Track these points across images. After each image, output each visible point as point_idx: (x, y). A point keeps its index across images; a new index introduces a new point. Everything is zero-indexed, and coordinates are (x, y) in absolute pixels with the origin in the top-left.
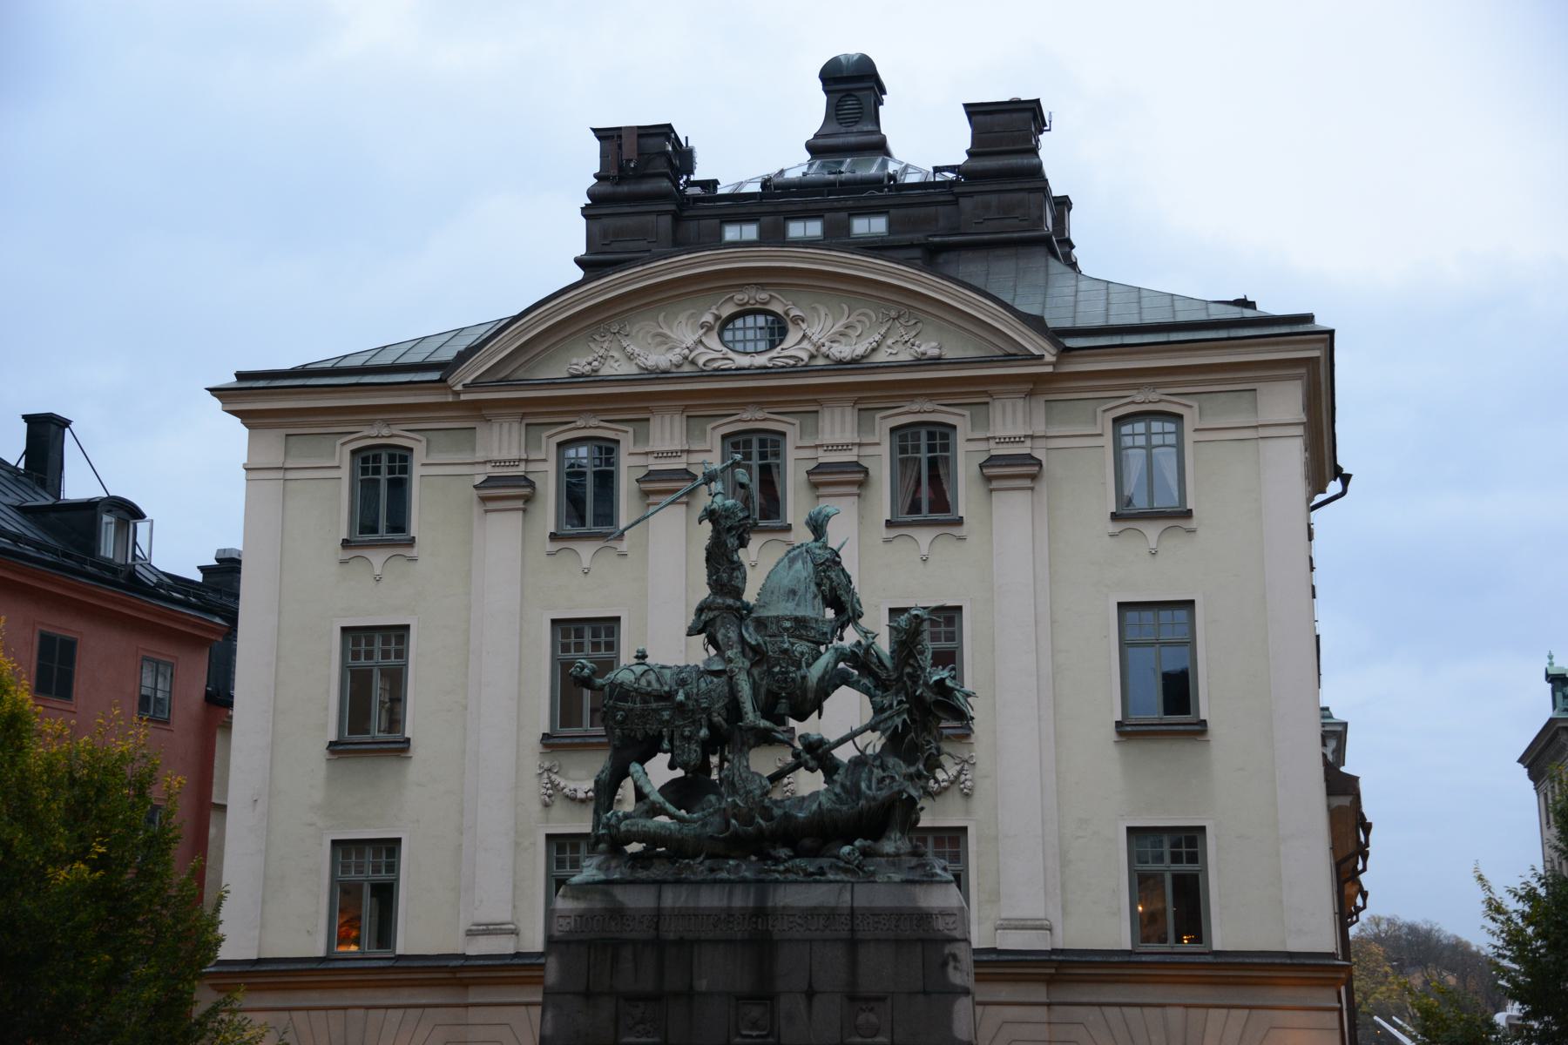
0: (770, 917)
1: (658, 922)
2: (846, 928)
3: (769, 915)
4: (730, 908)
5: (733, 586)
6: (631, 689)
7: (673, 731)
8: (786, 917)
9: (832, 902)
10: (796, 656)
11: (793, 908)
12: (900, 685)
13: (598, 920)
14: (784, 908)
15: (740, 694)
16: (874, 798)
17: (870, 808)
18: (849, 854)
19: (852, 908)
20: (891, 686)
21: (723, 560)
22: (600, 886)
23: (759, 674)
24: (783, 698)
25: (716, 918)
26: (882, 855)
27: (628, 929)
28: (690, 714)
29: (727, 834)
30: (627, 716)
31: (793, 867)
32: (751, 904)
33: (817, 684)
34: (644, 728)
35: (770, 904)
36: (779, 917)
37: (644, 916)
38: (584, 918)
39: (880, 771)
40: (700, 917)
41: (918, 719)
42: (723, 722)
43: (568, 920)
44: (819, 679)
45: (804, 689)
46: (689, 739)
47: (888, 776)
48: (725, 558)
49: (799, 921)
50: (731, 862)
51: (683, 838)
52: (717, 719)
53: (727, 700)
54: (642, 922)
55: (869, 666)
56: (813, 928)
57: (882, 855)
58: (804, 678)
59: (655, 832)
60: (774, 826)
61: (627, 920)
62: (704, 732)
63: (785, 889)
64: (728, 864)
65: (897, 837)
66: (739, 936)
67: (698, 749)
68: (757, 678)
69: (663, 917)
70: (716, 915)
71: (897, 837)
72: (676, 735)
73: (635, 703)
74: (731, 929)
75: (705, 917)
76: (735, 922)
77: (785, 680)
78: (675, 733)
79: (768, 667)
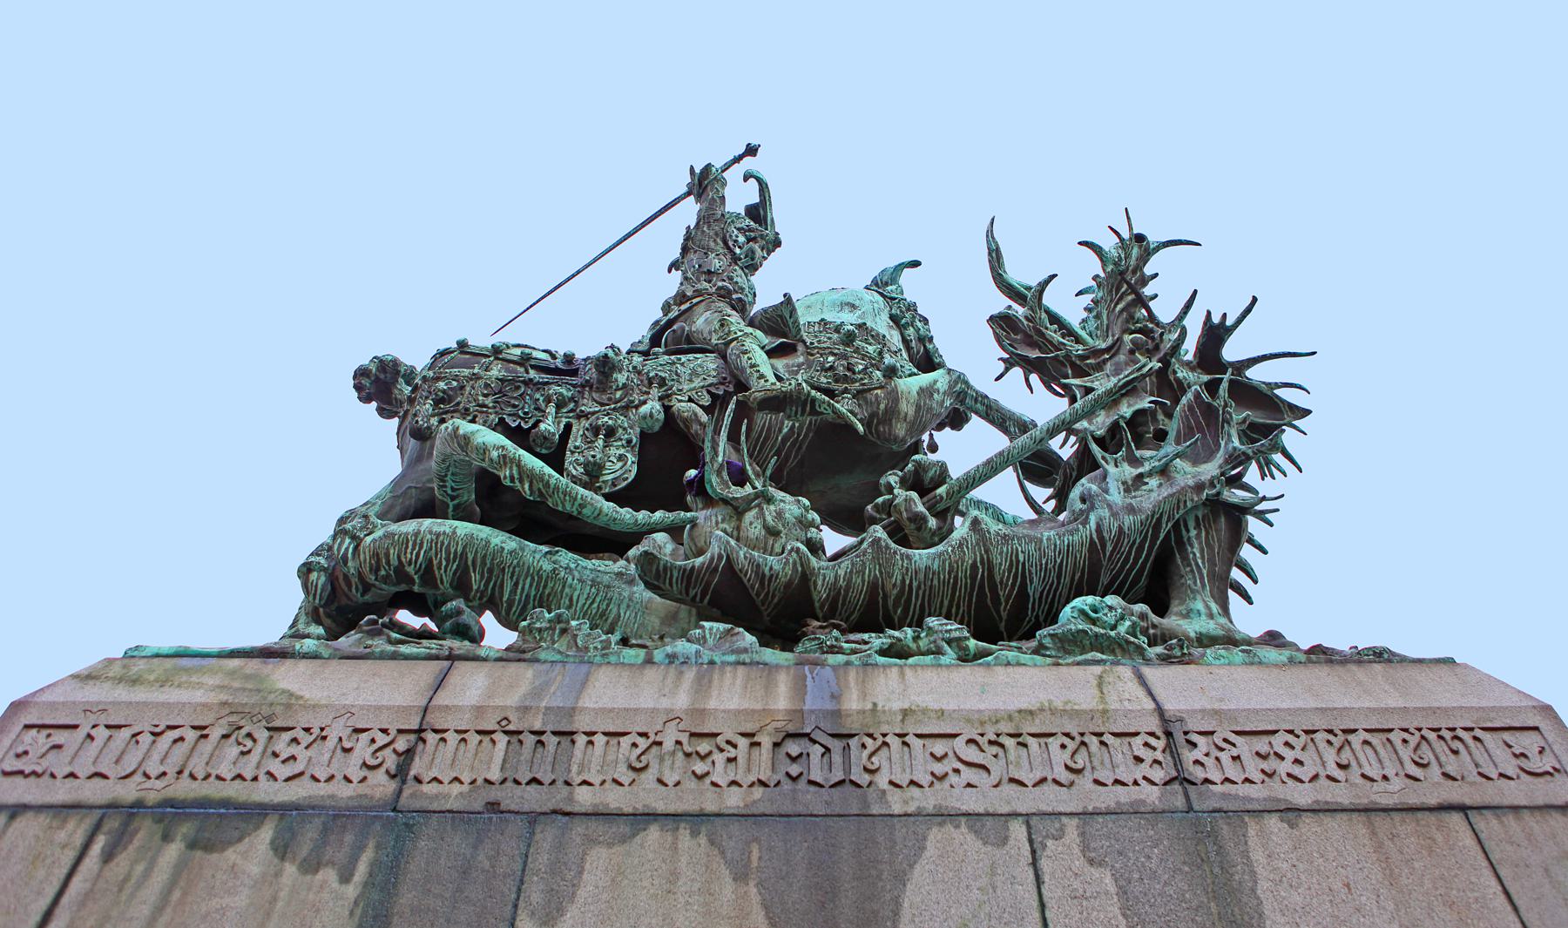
0: (853, 742)
1: (409, 753)
2: (1158, 775)
3: (852, 736)
4: (699, 713)
7: (568, 427)
8: (910, 739)
9: (1086, 699)
11: (941, 713)
12: (1122, 357)
13: (182, 739)
14: (905, 713)
15: (746, 356)
16: (1131, 510)
17: (1120, 529)
20: (1099, 367)
21: (717, 244)
22: (235, 663)
23: (787, 366)
25: (643, 743)
27: (283, 771)
28: (618, 394)
29: (700, 560)
31: (916, 638)
32: (782, 701)
34: (496, 413)
35: (852, 702)
36: (894, 742)
37: (358, 731)
38: (125, 734)
39: (1126, 466)
40: (581, 740)
42: (700, 412)
43: (59, 737)
45: (894, 397)
46: (610, 433)
47: (1150, 474)
48: (719, 241)
49: (971, 754)
50: (707, 624)
51: (554, 569)
52: (681, 406)
53: (710, 380)
54: (347, 751)
55: (1043, 335)
56: (1029, 778)
60: (841, 572)
61: (295, 740)
62: (653, 406)
63: (902, 674)
64: (702, 627)
66: (734, 800)
67: (629, 455)
69: (438, 736)
70: (644, 735)
72: (578, 428)
74: (700, 777)
75: (600, 740)
76: (719, 758)
77: (850, 368)
78: (574, 429)
79: (807, 360)
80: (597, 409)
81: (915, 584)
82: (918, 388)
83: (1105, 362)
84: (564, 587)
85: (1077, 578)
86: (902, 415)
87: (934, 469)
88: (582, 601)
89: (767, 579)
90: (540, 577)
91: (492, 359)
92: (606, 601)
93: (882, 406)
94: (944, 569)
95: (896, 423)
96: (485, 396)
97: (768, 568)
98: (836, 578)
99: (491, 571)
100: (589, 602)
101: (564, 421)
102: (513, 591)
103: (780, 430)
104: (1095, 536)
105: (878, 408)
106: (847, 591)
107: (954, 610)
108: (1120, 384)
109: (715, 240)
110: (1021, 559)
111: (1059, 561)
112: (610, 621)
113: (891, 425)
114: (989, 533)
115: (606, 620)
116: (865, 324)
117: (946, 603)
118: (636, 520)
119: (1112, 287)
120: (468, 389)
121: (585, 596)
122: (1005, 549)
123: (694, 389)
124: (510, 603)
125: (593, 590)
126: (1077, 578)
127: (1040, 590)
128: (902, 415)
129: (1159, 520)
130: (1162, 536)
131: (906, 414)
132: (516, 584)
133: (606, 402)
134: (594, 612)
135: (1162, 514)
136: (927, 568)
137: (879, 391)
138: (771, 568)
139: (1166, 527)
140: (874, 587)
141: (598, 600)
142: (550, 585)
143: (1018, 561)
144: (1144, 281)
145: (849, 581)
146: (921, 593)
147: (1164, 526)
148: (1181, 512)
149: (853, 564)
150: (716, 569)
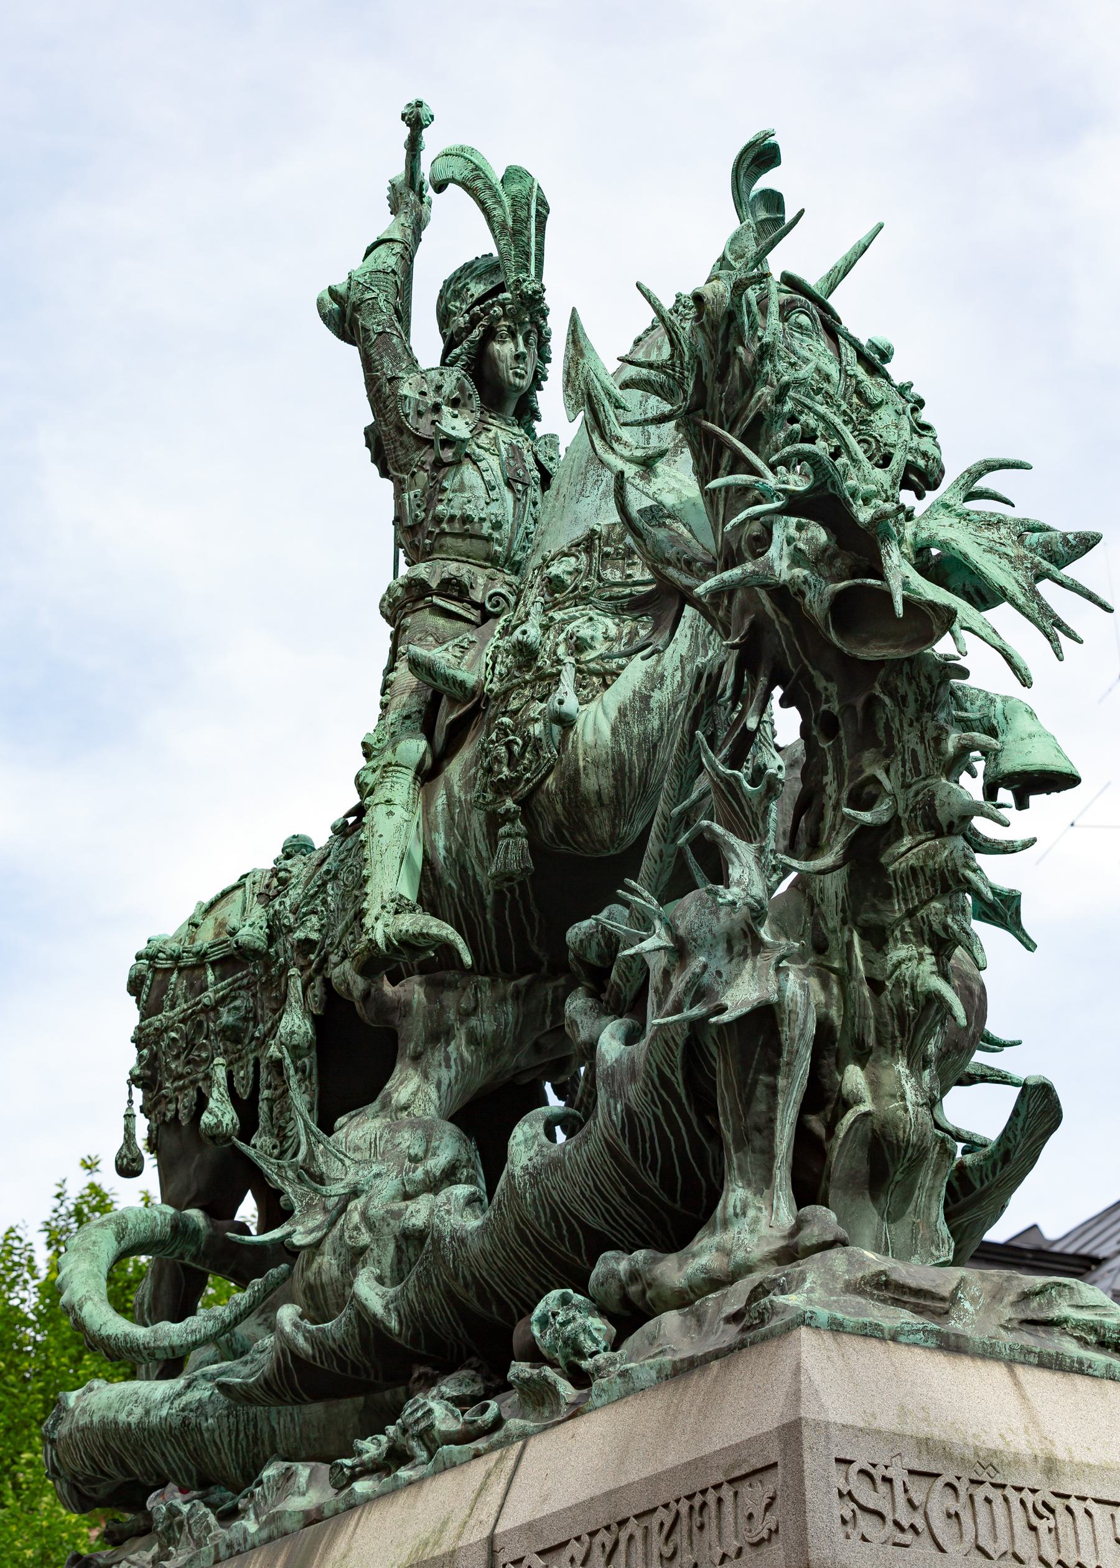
5: (438, 520)
6: (168, 964)
10: (559, 662)
17: (628, 1110)
18: (544, 1322)
19: (491, 1539)
23: (465, 771)
24: (508, 817)
26: (683, 1299)
30: (154, 1057)
33: (614, 731)
41: (835, 707)
44: (622, 712)
48: (405, 438)
57: (683, 1299)
58: (565, 722)
59: (102, 1420)
60: (411, 1295)
65: (731, 1210)
68: (456, 789)
71: (731, 1210)
73: (173, 1007)
80: (269, 1024)
81: (484, 1274)
82: (613, 714)
83: (728, 610)
84: (202, 1434)
85: (624, 1192)
86: (593, 798)
87: (594, 944)
88: (226, 1440)
89: (338, 1351)
90: (175, 1437)
91: (175, 975)
92: (252, 1423)
93: (559, 807)
94: (496, 1245)
95: (592, 818)
96: (177, 1057)
97: (331, 1342)
98: (409, 1305)
99: (136, 1452)
100: (233, 1437)
101: (251, 1057)
102: (166, 1461)
103: (483, 907)
104: (606, 1135)
105: (557, 814)
106: (429, 1314)
107: (544, 1281)
108: (686, 727)
109: (402, 444)
110: (557, 1198)
111: (591, 1183)
112: (267, 1443)
113: (587, 827)
114: (513, 1177)
115: (263, 1443)
116: (593, 531)
117: (528, 1278)
118: (223, 1321)
119: (700, 444)
120: (161, 1054)
121: (226, 1432)
122: (536, 1194)
123: (347, 927)
124: (172, 1471)
125: (232, 1419)
126: (624, 1192)
127: (603, 1222)
128: (593, 798)
129: (661, 1074)
130: (681, 1091)
131: (599, 794)
132: (163, 1454)
133: (274, 1006)
134: (244, 1444)
135: (658, 1067)
136: (482, 1251)
137: (550, 780)
138: (334, 1340)
139: (678, 1079)
140: (450, 1295)
141: (241, 1428)
142: (189, 1440)
143: (555, 1201)
144: (751, 379)
145: (423, 1301)
146: (497, 1279)
147: (673, 1078)
148: (678, 1053)
149: (418, 1278)
150: (286, 1363)
